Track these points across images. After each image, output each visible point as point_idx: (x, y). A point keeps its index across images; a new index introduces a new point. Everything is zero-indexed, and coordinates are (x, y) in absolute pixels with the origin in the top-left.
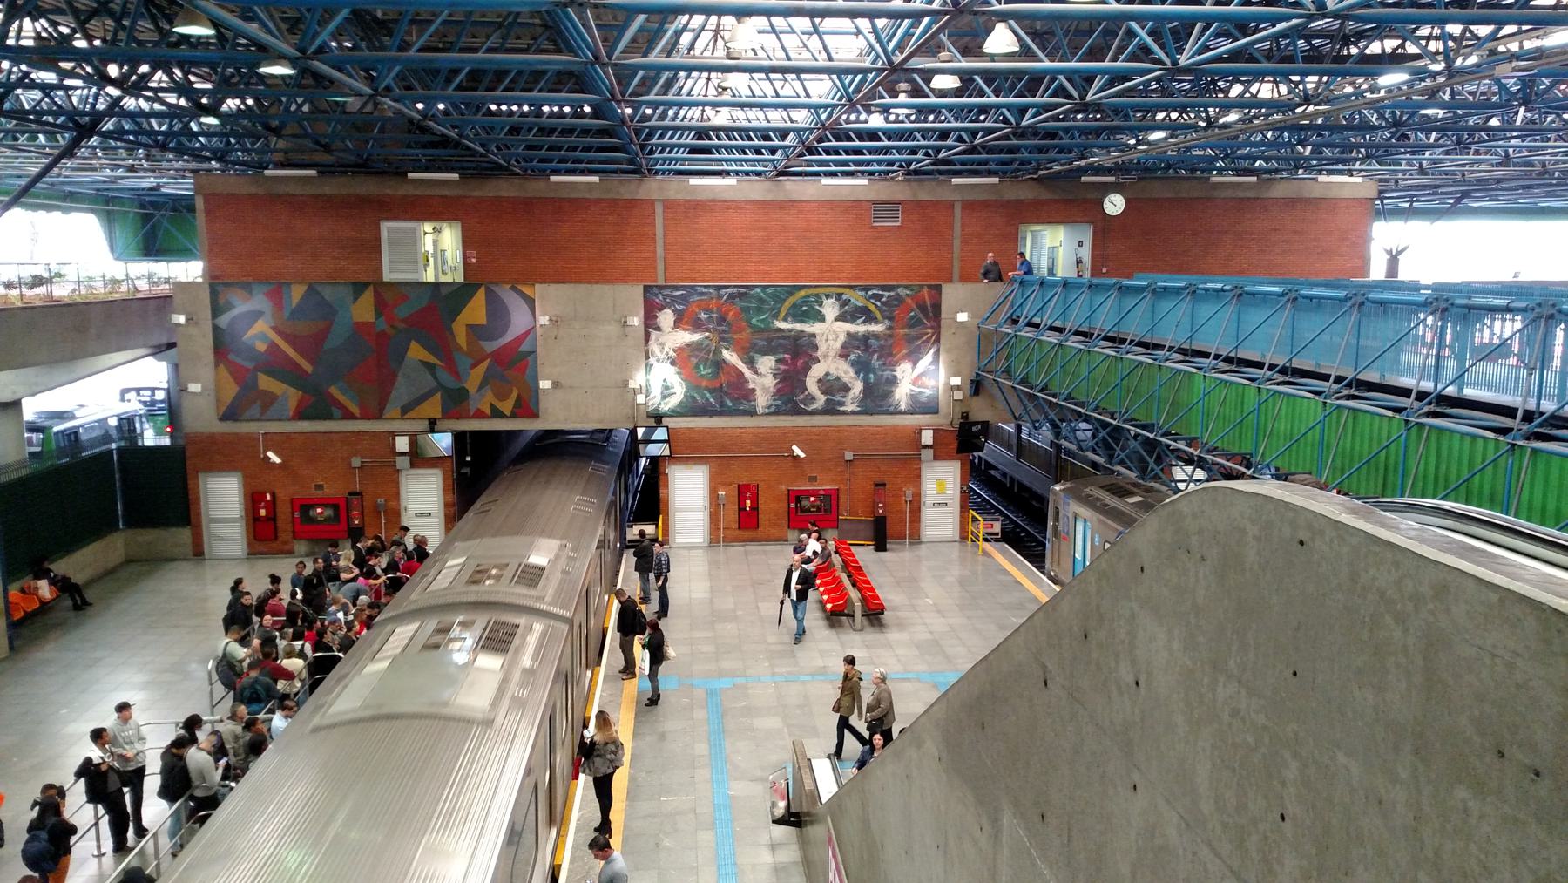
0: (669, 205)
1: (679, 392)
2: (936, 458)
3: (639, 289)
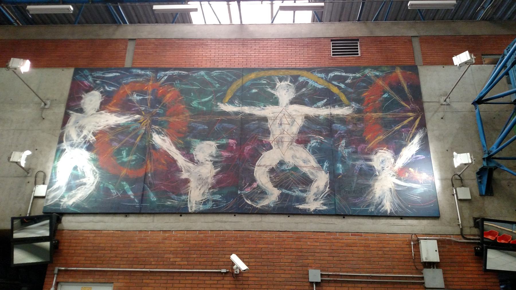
1: (91, 179)
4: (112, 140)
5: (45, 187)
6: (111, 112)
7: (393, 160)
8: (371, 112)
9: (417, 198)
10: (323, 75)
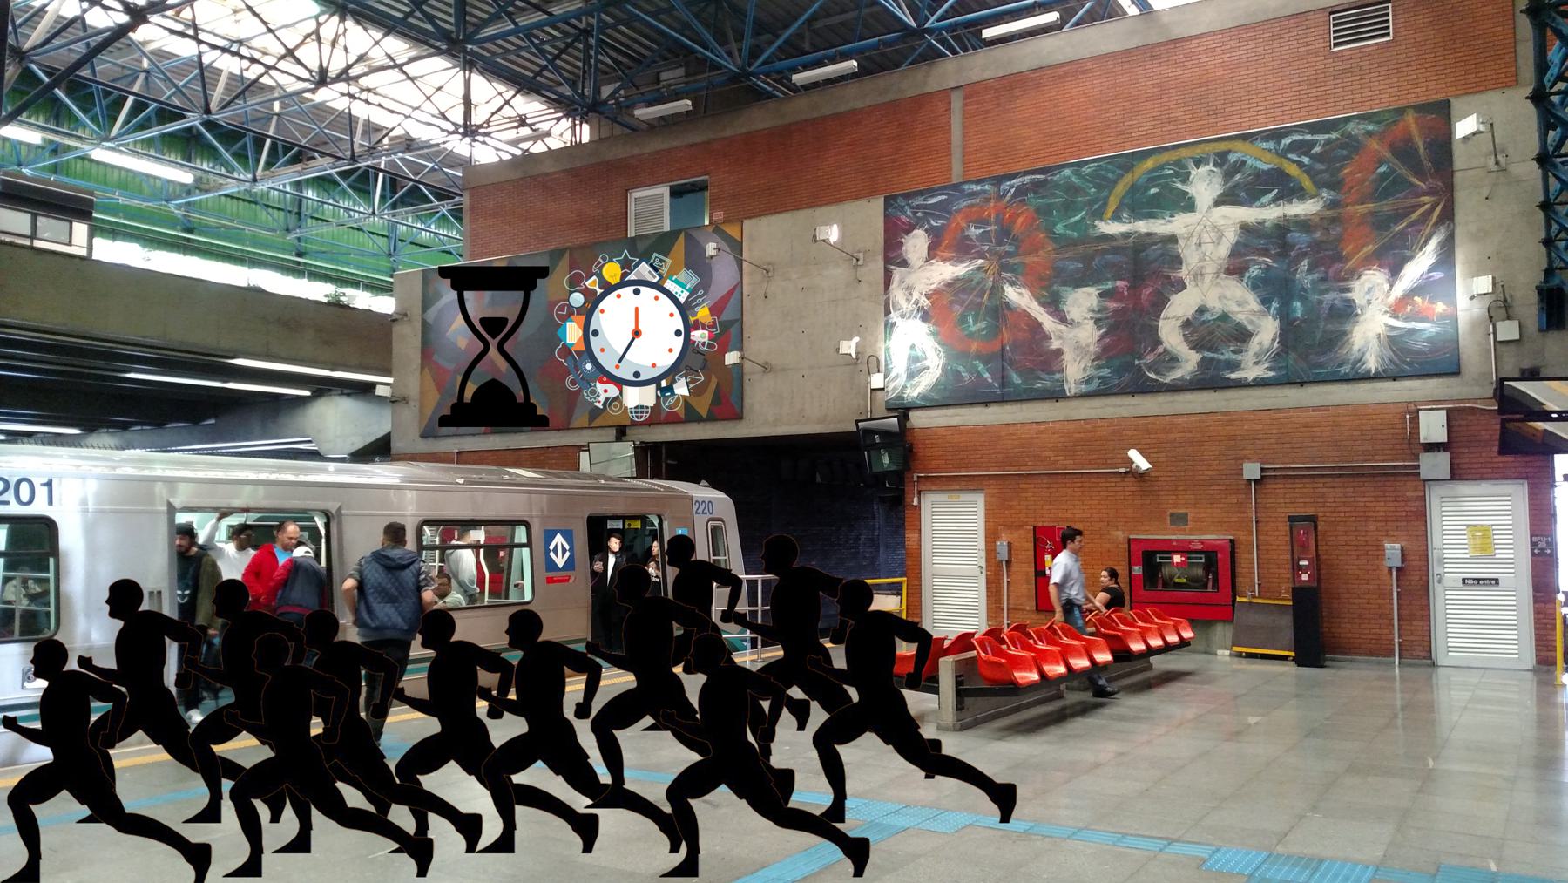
0: (972, 91)
2: (1457, 474)
3: (876, 206)
4: (951, 303)
5: (881, 376)
6: (944, 260)
7: (1387, 286)
8: (1353, 204)
9: (1420, 345)
10: (1271, 145)
